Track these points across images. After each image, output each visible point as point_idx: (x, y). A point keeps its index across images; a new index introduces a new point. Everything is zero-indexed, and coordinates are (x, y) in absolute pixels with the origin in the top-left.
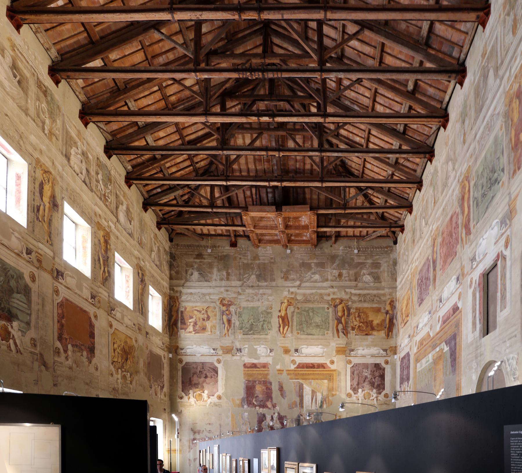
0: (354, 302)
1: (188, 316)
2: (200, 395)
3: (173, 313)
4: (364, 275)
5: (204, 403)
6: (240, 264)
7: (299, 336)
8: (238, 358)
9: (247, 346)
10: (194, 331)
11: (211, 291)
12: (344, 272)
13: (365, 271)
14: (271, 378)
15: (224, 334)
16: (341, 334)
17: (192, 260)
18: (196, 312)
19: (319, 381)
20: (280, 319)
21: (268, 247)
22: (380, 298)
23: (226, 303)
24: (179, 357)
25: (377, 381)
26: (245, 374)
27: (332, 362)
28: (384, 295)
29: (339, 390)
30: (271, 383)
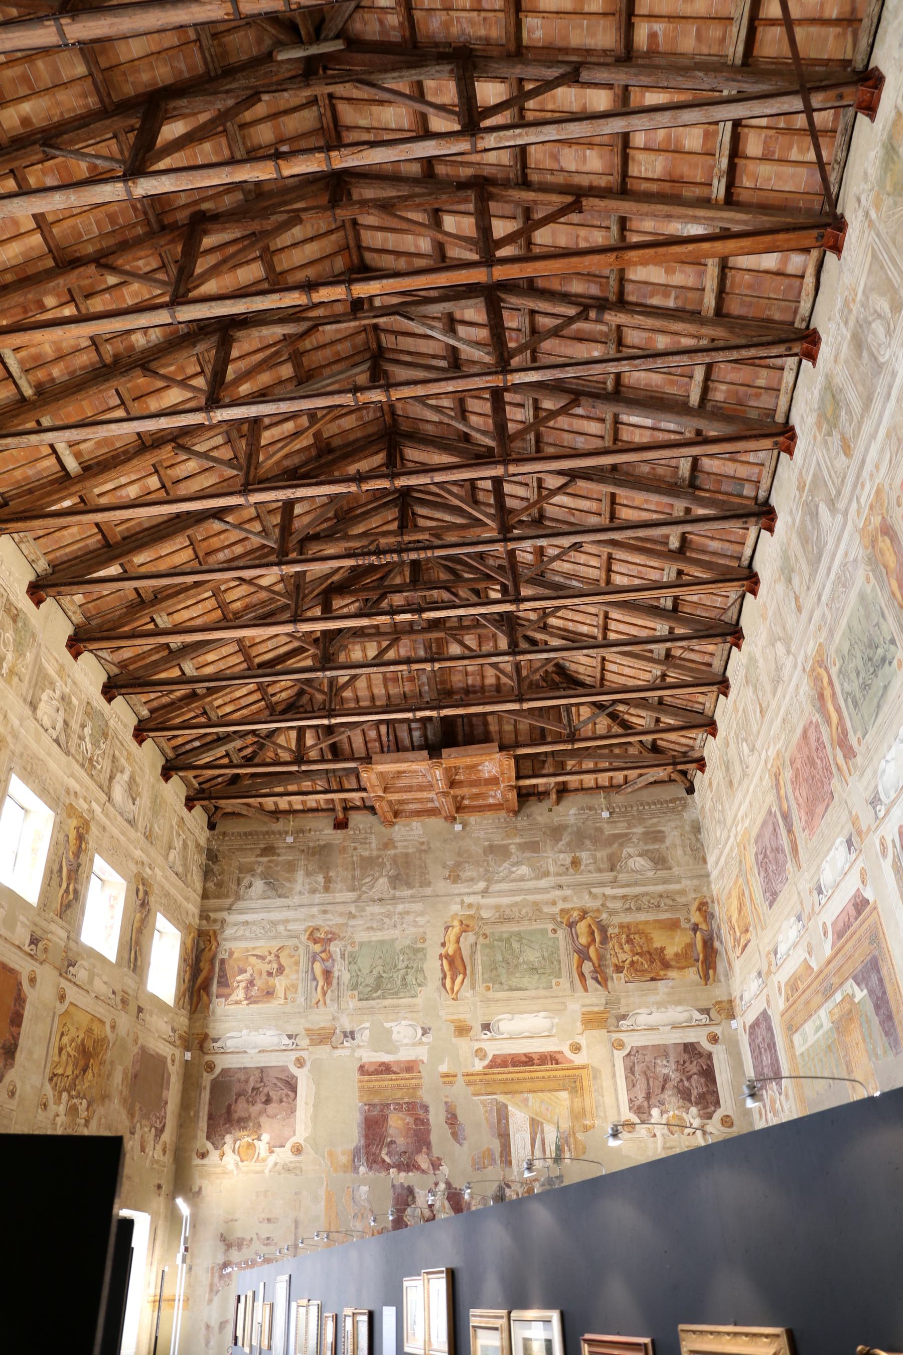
0: (612, 913)
1: (236, 969)
2: (250, 1146)
3: (202, 965)
4: (630, 856)
5: (256, 1166)
6: (355, 859)
7: (490, 994)
8: (347, 1052)
9: (367, 1025)
10: (246, 999)
11: (290, 914)
12: (584, 855)
13: (630, 850)
14: (425, 1096)
15: (314, 1001)
16: (590, 982)
17: (253, 859)
18: (253, 960)
19: (546, 1096)
20: (445, 961)
21: (414, 824)
22: (673, 900)
23: (322, 936)
24: (208, 1058)
25: (697, 1086)
26: (361, 1089)
27: (576, 1048)
28: (682, 892)
29: (602, 1114)
30: (426, 1108)
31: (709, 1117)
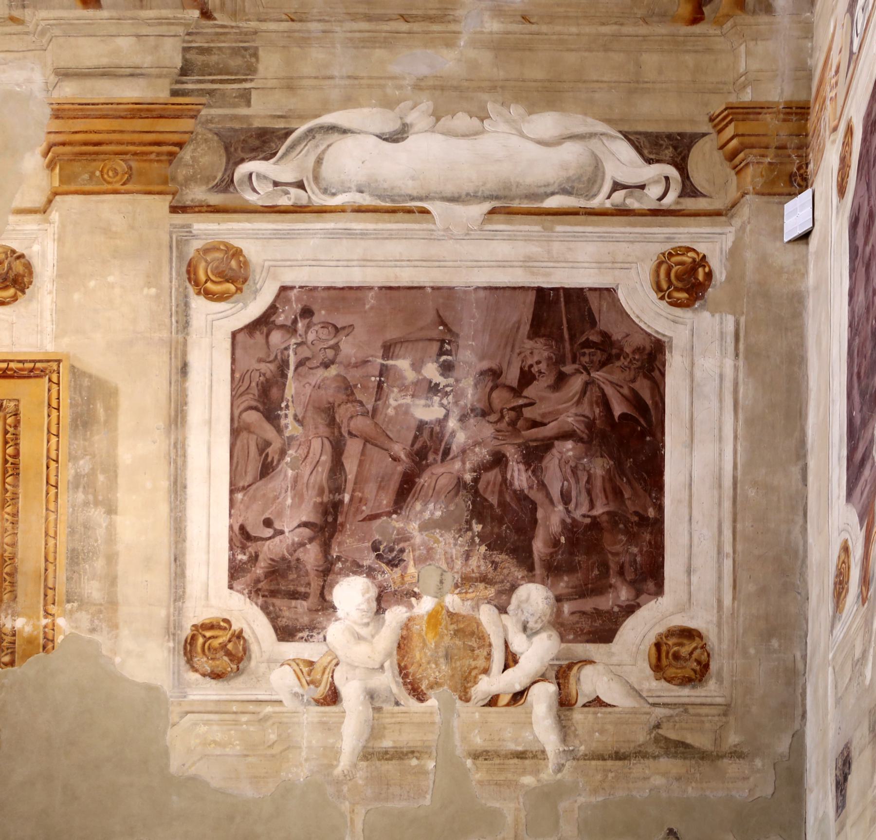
25: (566, 489)
29: (93, 590)
31: (603, 630)
